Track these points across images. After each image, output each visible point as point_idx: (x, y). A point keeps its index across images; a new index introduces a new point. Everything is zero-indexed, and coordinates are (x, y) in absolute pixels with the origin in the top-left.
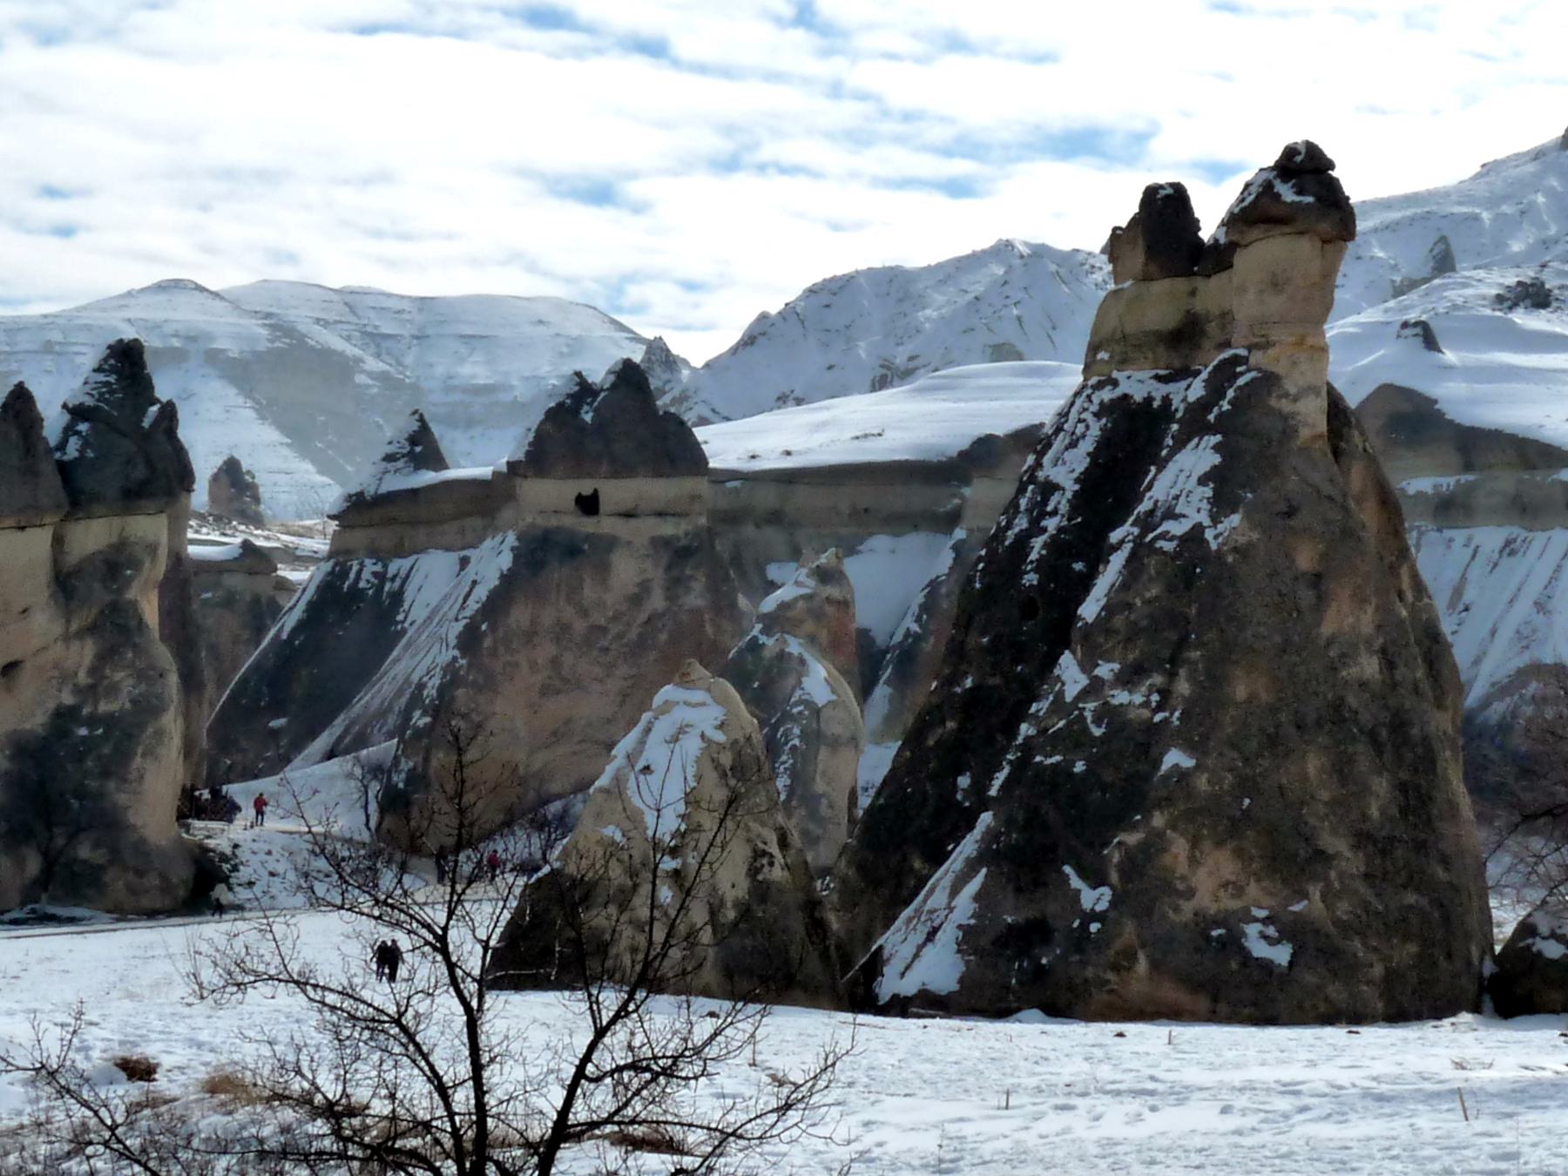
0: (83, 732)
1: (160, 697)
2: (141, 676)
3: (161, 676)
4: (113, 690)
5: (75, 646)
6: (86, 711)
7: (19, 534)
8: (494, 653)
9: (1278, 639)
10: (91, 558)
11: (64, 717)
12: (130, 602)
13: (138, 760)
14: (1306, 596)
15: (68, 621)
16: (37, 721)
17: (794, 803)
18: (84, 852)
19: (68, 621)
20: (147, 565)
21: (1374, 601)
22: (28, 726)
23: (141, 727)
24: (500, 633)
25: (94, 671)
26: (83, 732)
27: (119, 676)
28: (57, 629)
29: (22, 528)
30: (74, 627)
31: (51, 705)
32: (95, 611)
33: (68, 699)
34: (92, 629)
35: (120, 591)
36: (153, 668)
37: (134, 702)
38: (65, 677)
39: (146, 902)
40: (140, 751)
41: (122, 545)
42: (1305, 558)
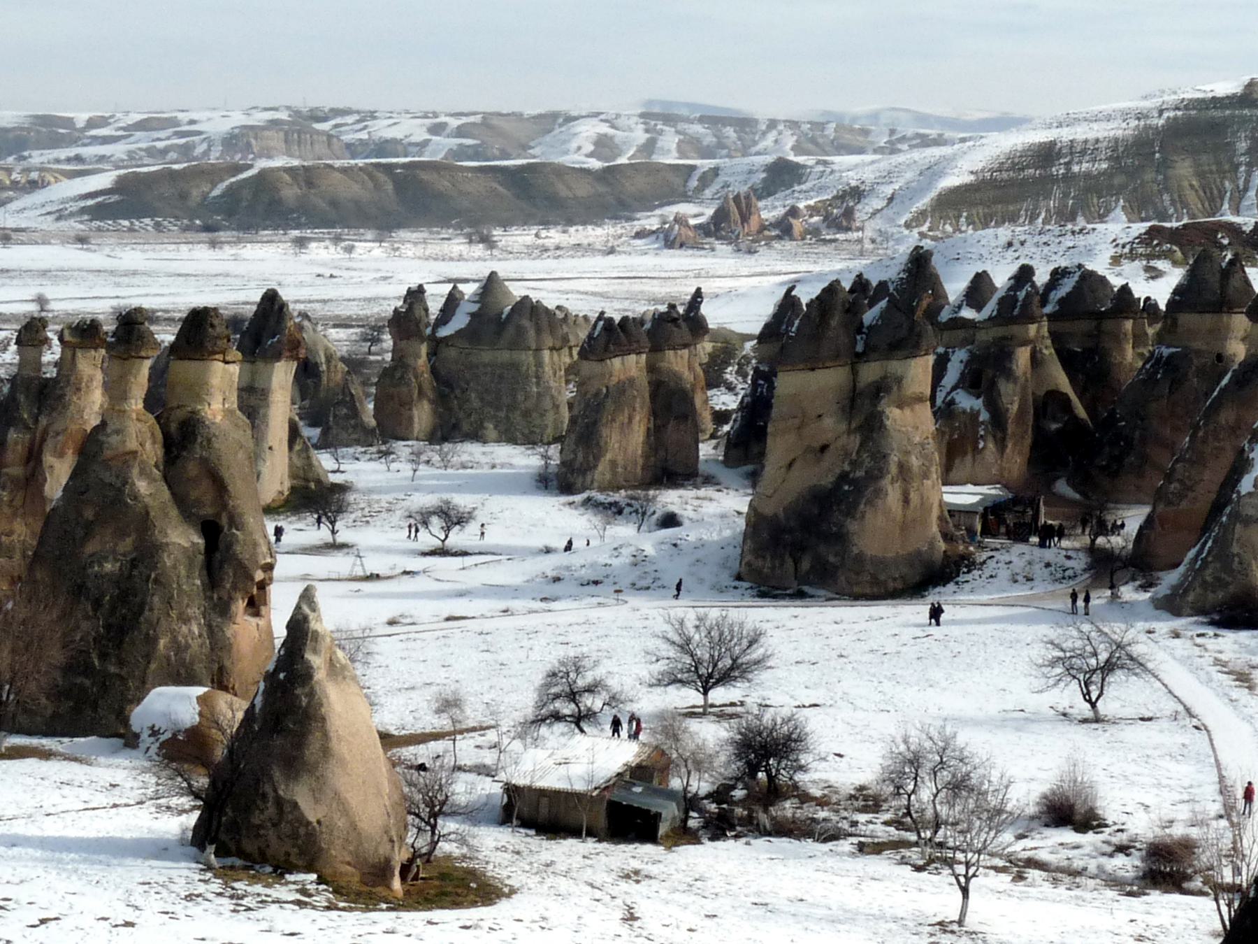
0: (846, 488)
1: (881, 470)
2: (873, 457)
3: (884, 457)
4: (862, 463)
5: (852, 438)
6: (851, 475)
7: (811, 373)
8: (1204, 441)
9: (57, 553)
10: (869, 385)
11: (843, 477)
12: (879, 412)
13: (862, 506)
14: (80, 532)
15: (850, 424)
16: (828, 480)
17: (1210, 559)
18: (832, 559)
19: (850, 424)
20: (895, 388)
21: (134, 536)
22: (823, 483)
23: (867, 487)
24: (1211, 427)
25: (858, 452)
26: (846, 488)
27: (865, 455)
28: (843, 427)
29: (813, 369)
30: (854, 425)
31: (838, 471)
32: (863, 417)
33: (847, 467)
34: (860, 428)
35: (875, 406)
36: (879, 452)
37: (866, 472)
38: (847, 454)
39: (856, 589)
40: (864, 500)
41: (884, 378)
42: (89, 514)
